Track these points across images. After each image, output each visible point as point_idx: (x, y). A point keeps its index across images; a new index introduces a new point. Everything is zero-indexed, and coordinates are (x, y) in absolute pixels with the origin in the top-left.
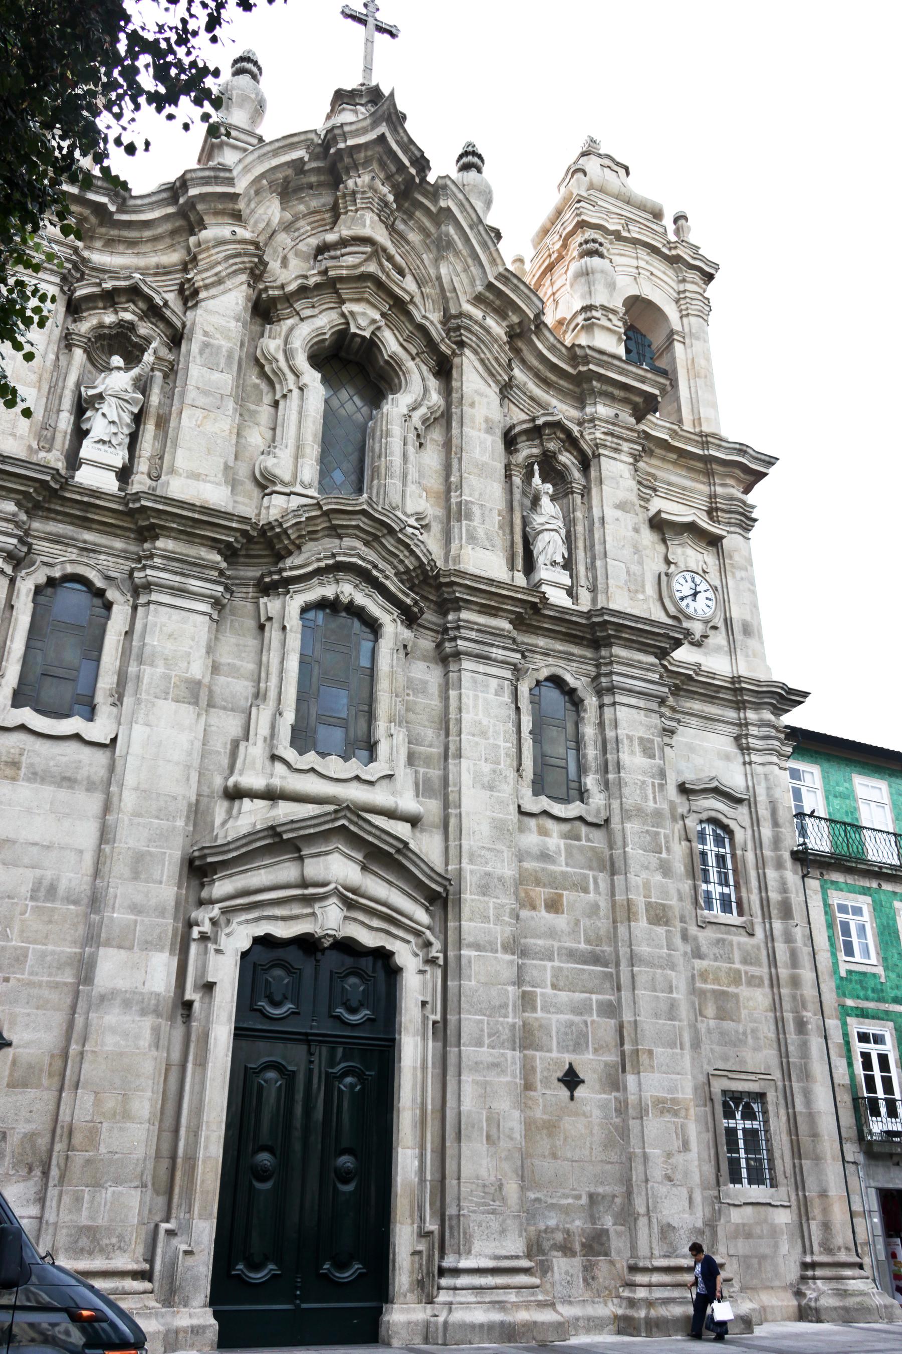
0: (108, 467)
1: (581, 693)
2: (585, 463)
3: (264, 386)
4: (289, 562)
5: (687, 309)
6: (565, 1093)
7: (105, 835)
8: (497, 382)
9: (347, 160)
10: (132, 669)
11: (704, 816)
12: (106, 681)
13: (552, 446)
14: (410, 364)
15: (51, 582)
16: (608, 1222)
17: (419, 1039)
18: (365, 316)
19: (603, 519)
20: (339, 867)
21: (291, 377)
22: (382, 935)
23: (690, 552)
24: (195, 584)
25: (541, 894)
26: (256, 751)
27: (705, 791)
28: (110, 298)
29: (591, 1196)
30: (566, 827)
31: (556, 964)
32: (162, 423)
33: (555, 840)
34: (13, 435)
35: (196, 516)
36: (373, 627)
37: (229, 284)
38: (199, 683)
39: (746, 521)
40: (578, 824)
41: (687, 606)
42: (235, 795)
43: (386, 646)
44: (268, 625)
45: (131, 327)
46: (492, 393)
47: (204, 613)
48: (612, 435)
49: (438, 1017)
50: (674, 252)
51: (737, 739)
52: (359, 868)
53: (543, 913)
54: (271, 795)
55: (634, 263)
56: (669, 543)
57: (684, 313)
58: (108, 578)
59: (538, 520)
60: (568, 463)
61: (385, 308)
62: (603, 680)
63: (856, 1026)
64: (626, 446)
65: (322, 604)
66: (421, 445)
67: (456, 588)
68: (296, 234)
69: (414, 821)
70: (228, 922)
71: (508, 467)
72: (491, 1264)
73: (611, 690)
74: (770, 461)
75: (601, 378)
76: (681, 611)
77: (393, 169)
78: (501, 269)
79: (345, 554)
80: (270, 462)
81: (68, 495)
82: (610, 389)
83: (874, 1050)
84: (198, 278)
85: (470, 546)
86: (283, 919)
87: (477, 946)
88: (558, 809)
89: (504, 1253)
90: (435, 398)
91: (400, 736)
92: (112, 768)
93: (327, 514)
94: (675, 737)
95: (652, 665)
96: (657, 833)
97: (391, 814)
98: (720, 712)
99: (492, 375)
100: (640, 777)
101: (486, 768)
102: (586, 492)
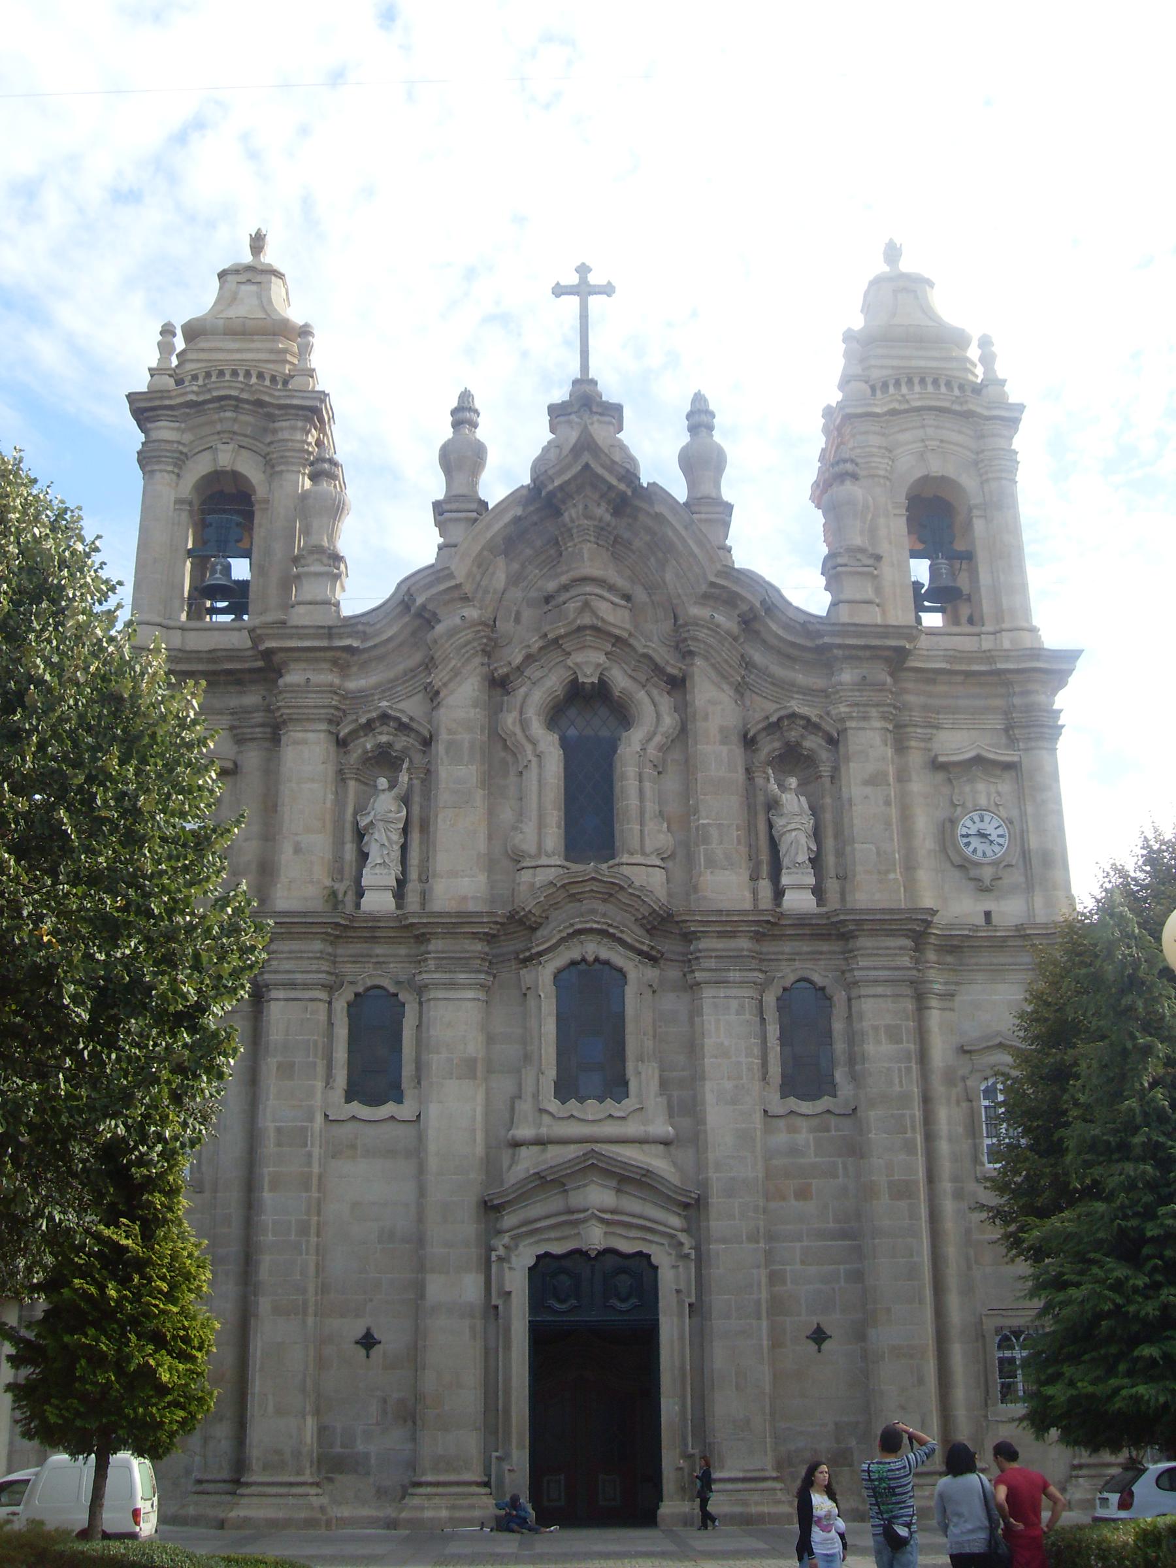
1: (828, 991)
2: (833, 742)
3: (510, 759)
4: (539, 933)
5: (986, 473)
7: (422, 1192)
8: (730, 684)
9: (559, 495)
13: (793, 735)
14: (641, 695)
15: (357, 995)
16: (853, 1443)
17: (675, 1319)
18: (590, 662)
19: (850, 800)
20: (598, 1195)
21: (529, 748)
22: (641, 1242)
23: (981, 786)
24: (462, 976)
28: (369, 726)
29: (836, 1424)
30: (815, 1122)
31: (805, 1244)
32: (425, 826)
33: (804, 1136)
34: (311, 882)
35: (453, 920)
38: (475, 1060)
40: (827, 1116)
41: (975, 850)
43: (630, 991)
44: (528, 992)
45: (390, 745)
47: (474, 999)
48: (857, 705)
49: (693, 1300)
50: (965, 408)
52: (613, 1193)
53: (793, 1202)
54: (541, 1142)
56: (955, 783)
57: (984, 477)
58: (398, 983)
59: (779, 822)
61: (609, 648)
62: (848, 975)
64: (873, 712)
65: (573, 963)
66: (659, 773)
67: (689, 924)
68: (525, 584)
69: (666, 1143)
70: (517, 1246)
71: (748, 771)
72: (741, 1475)
73: (856, 983)
74: (1072, 656)
75: (840, 646)
76: (966, 859)
77: (605, 489)
78: (719, 567)
79: (581, 922)
81: (356, 925)
82: (854, 652)
84: (437, 678)
85: (709, 871)
86: (557, 1239)
87: (724, 1241)
88: (805, 1107)
89: (751, 1467)
92: (421, 1138)
93: (563, 886)
94: (957, 998)
95: (901, 948)
96: (903, 1115)
98: (1010, 960)
99: (724, 677)
100: (886, 1065)
101: (728, 1085)
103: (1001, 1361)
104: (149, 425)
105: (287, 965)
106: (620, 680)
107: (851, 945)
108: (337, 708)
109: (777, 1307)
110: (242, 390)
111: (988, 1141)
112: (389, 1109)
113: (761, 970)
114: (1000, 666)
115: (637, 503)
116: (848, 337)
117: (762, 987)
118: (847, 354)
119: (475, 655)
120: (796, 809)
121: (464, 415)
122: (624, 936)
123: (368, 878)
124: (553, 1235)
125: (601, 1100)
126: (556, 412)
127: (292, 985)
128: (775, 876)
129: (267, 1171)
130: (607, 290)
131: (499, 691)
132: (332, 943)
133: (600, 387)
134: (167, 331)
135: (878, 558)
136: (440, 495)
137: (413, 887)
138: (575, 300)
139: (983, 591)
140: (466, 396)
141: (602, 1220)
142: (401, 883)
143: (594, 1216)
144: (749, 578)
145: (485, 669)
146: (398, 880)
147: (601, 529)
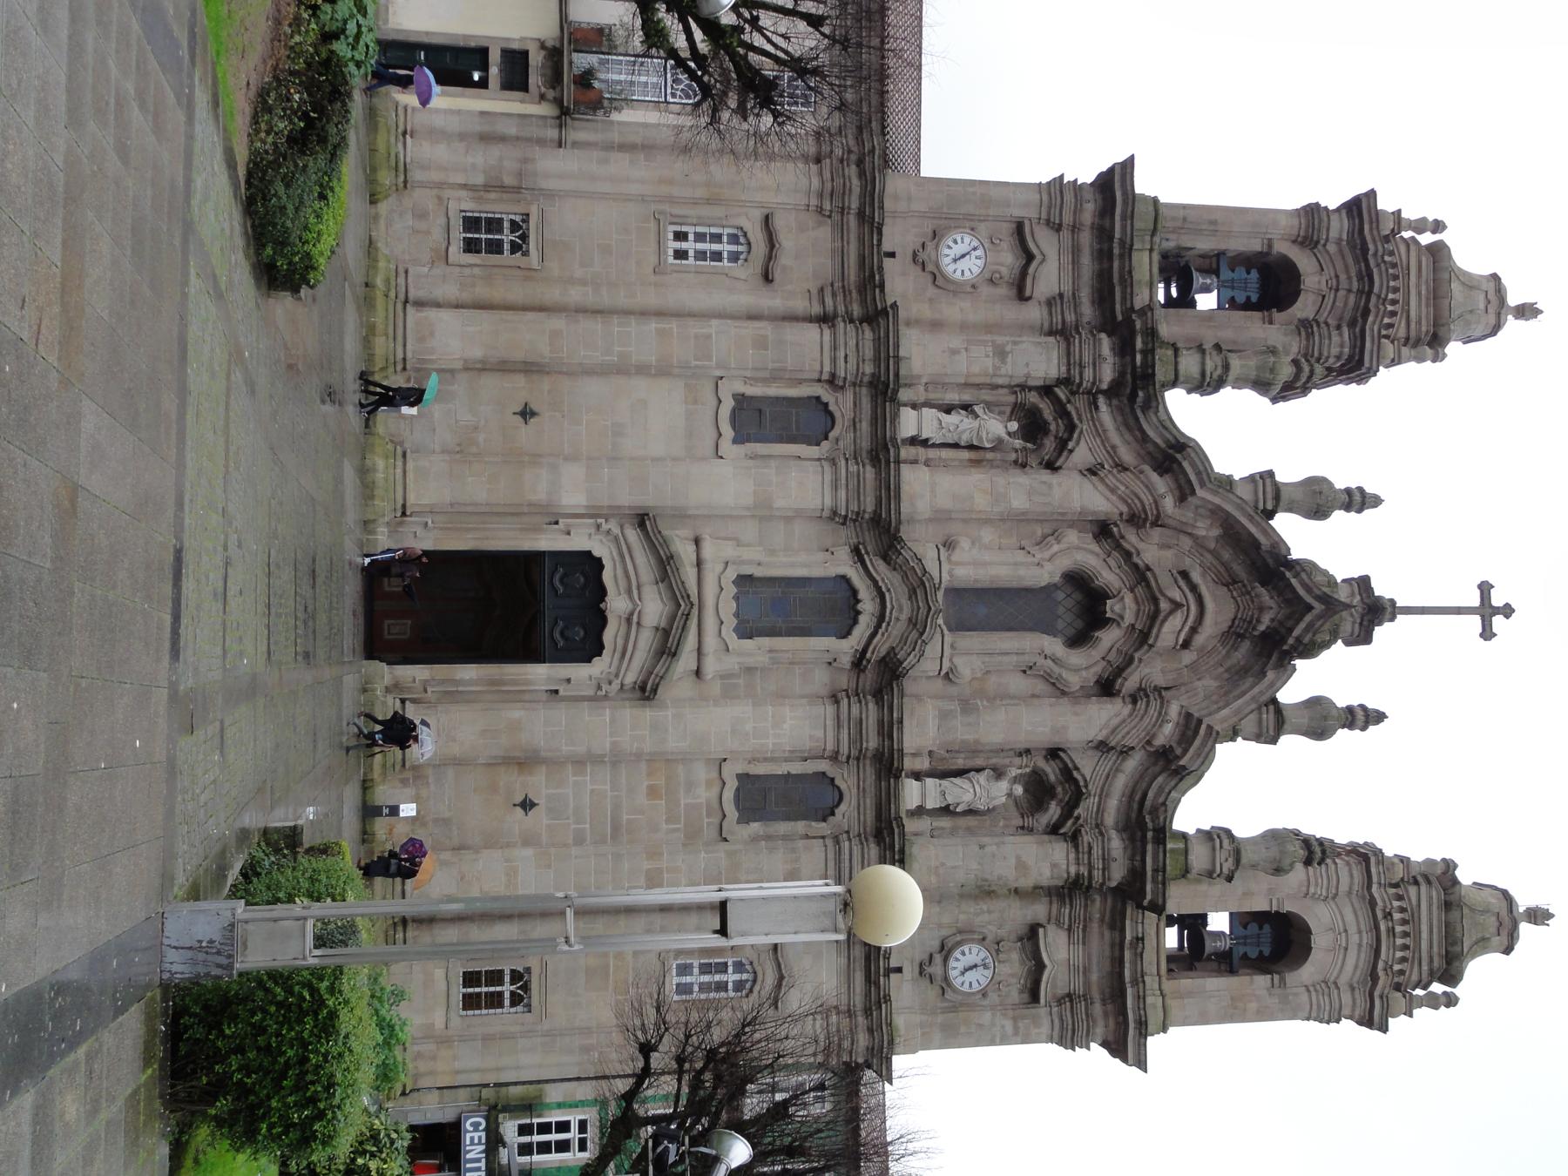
0: (920, 428)
2: (1054, 830)
6: (519, 799)
10: (773, 463)
11: (759, 969)
12: (761, 448)
15: (826, 405)
18: (1124, 607)
20: (654, 609)
21: (1047, 555)
24: (842, 494)
25: (661, 781)
26: (729, 551)
27: (779, 966)
28: (1062, 413)
32: (976, 463)
33: (704, 795)
36: (845, 634)
37: (1114, 498)
39: (1070, 1038)
40: (720, 816)
42: (697, 541)
45: (1046, 432)
46: (1095, 732)
49: (561, 693)
50: (1381, 973)
51: (836, 1007)
54: (699, 564)
55: (1352, 929)
59: (982, 778)
60: (1051, 811)
61: (1139, 627)
63: (591, 1115)
64: (1084, 871)
65: (854, 592)
71: (1028, 751)
74: (1141, 1064)
75: (1144, 837)
76: (950, 952)
80: (965, 543)
83: (573, 1135)
87: (613, 721)
88: (729, 795)
90: (1074, 681)
91: (762, 659)
92: (704, 459)
93: (923, 583)
97: (699, 651)
99: (1113, 731)
101: (749, 727)
102: (1026, 830)
103: (501, 972)
104: (1344, 213)
105: (852, 343)
106: (1109, 638)
107: (871, 839)
108: (1080, 384)
109: (554, 763)
110: (1379, 297)
111: (696, 964)
112: (728, 432)
113: (849, 757)
114: (1129, 991)
115: (1274, 658)
116: (1449, 866)
117: (834, 757)
118: (1430, 862)
119: (1129, 505)
120: (994, 793)
121: (1358, 500)
122: (879, 636)
123: (929, 414)
124: (620, 572)
125: (737, 615)
126: (1364, 583)
127: (835, 348)
128: (933, 774)
129: (673, 325)
130: (1487, 633)
131: (1095, 529)
132: (871, 383)
133: (1387, 624)
134: (1438, 226)
135: (1230, 879)
136: (1280, 478)
137: (921, 452)
138: (1476, 602)
139: (1199, 981)
140: (1376, 501)
141: (632, 614)
142: (925, 443)
143: (635, 605)
144: (1207, 758)
145: (1116, 517)
146: (927, 440)
147: (1252, 623)
